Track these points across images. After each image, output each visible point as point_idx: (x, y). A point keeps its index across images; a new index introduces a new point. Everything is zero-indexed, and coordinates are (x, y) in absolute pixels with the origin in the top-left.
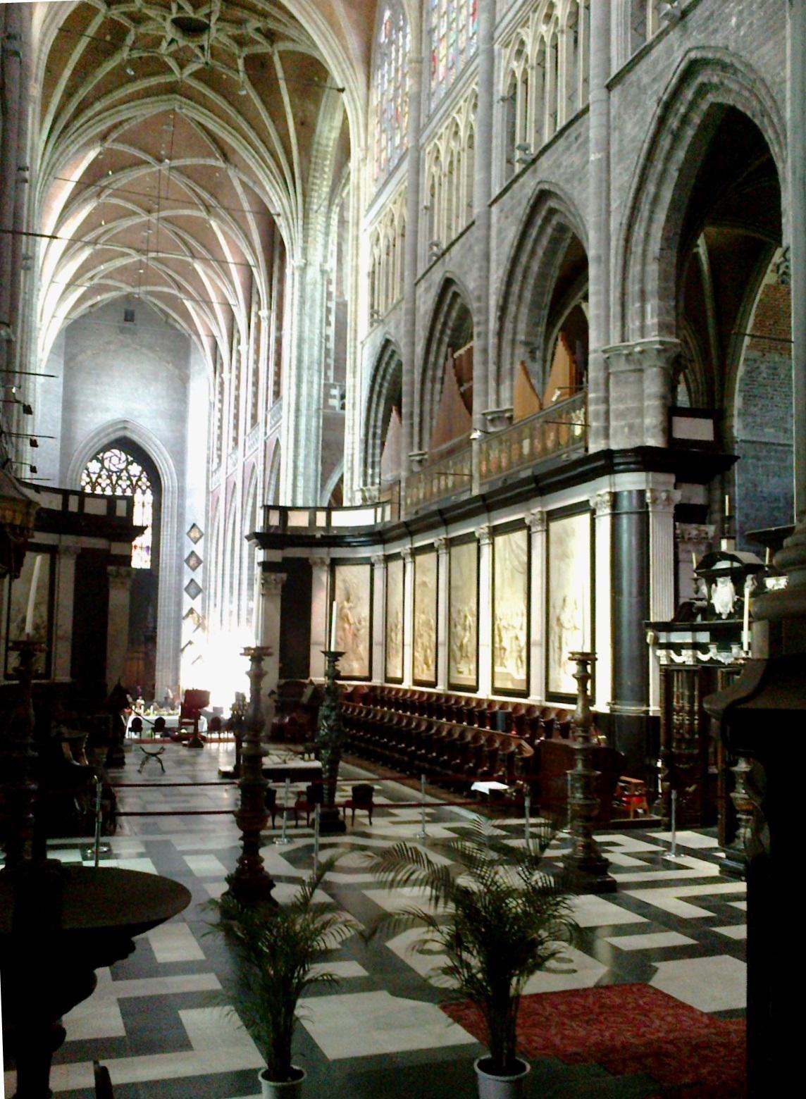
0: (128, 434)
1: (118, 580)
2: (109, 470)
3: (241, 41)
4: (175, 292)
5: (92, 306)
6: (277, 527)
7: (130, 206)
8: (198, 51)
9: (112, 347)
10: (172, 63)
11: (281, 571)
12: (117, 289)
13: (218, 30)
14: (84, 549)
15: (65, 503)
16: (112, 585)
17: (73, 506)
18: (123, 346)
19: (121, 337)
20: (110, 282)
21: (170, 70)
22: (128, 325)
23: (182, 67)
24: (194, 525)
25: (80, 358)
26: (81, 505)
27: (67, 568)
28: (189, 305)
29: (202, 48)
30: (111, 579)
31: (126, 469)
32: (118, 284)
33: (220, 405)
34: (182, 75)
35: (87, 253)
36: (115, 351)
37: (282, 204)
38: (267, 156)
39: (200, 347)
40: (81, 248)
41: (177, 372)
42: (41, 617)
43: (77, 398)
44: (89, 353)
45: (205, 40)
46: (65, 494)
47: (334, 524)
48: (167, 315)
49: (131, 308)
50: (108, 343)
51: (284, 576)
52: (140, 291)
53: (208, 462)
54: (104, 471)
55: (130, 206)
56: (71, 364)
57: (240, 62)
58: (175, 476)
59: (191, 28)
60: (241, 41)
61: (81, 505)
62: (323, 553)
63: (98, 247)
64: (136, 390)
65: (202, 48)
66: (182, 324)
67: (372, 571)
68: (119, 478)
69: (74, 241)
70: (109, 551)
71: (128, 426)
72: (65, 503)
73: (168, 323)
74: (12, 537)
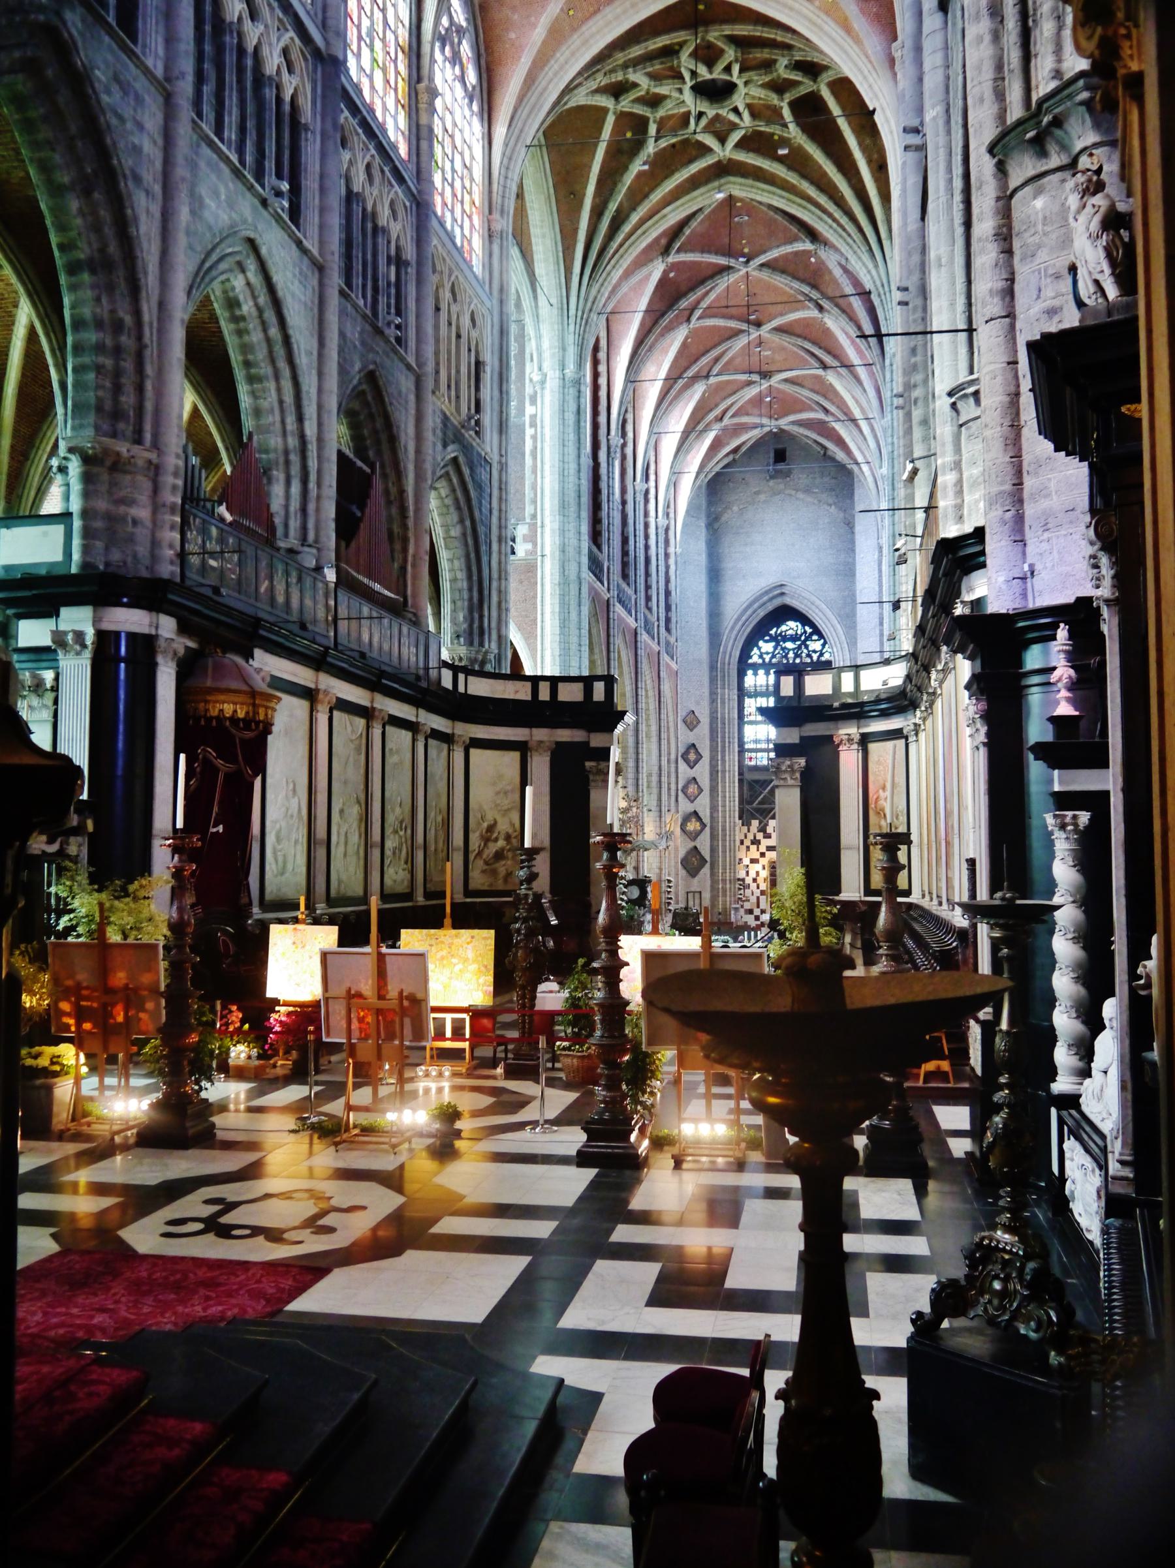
0: (788, 601)
1: (598, 778)
3: (780, 87)
4: (821, 415)
5: (735, 451)
6: (790, 697)
7: (733, 324)
8: (733, 117)
9: (762, 497)
10: (709, 141)
11: (800, 755)
12: (755, 426)
13: (746, 83)
14: (559, 744)
15: (535, 691)
16: (592, 784)
17: (544, 694)
18: (775, 494)
19: (771, 483)
20: (745, 419)
21: (707, 150)
22: (781, 466)
23: (722, 140)
25: (724, 519)
26: (554, 691)
27: (540, 766)
28: (837, 426)
29: (736, 110)
30: (591, 777)
32: (757, 420)
34: (726, 152)
35: (698, 391)
36: (765, 502)
37: (872, 277)
38: (844, 220)
40: (687, 387)
41: (842, 515)
42: (513, 825)
44: (735, 508)
45: (739, 100)
46: (535, 680)
47: (863, 687)
48: (825, 448)
49: (780, 446)
50: (757, 493)
51: (802, 762)
52: (784, 423)
55: (733, 324)
56: (716, 526)
57: (787, 113)
59: (716, 92)
60: (780, 87)
61: (554, 691)
62: (849, 730)
63: (712, 380)
64: (793, 545)
65: (736, 110)
66: (840, 455)
67: (414, 740)
69: (671, 380)
70: (588, 743)
72: (535, 691)
73: (826, 456)
74: (234, 731)
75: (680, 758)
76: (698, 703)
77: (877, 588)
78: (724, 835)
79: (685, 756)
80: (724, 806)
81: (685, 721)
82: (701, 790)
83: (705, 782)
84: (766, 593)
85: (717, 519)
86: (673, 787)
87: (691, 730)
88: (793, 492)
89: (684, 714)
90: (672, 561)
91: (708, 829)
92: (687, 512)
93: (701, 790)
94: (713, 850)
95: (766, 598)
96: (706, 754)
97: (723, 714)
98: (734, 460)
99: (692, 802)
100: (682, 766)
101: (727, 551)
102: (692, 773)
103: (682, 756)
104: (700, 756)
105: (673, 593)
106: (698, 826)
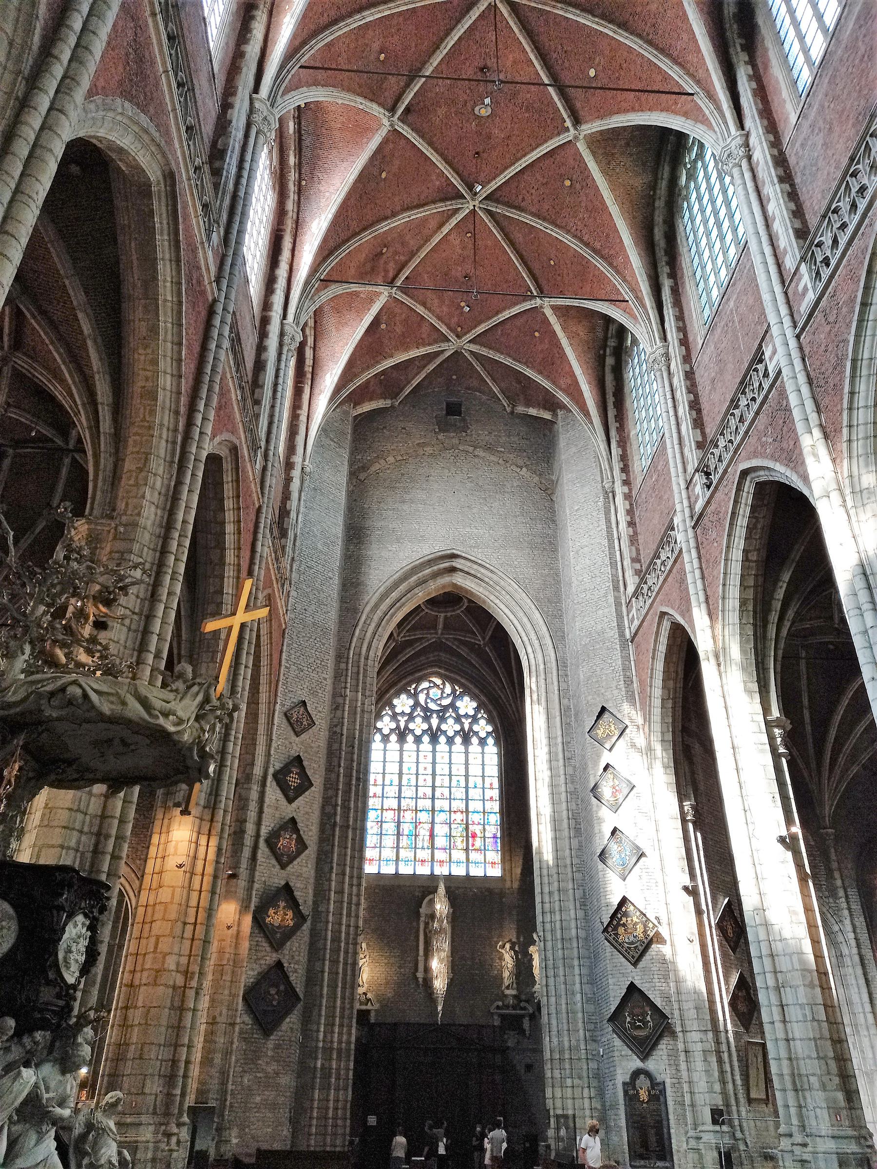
0: (459, 579)
2: (426, 709)
9: (429, 450)
24: (603, 710)
31: (452, 705)
33: (626, 489)
39: (575, 410)
41: (536, 479)
43: (368, 523)
44: (391, 459)
49: (453, 399)
53: (616, 588)
54: (419, 711)
56: (362, 476)
58: (548, 641)
68: (442, 719)
71: (458, 563)
75: (270, 778)
76: (313, 693)
77: (605, 542)
78: (336, 951)
79: (280, 778)
80: (340, 892)
81: (287, 716)
82: (302, 846)
83: (311, 832)
84: (430, 562)
85: (364, 468)
86: (250, 828)
87: (297, 734)
88: (471, 449)
89: (288, 704)
90: (296, 473)
91: (307, 927)
92: (324, 430)
93: (302, 846)
94: (312, 978)
95: (428, 571)
96: (317, 779)
97: (351, 732)
98: (392, 407)
99: (283, 866)
100: (273, 793)
101: (375, 507)
102: (289, 810)
103: (275, 776)
104: (306, 784)
105: (293, 515)
106: (289, 919)
